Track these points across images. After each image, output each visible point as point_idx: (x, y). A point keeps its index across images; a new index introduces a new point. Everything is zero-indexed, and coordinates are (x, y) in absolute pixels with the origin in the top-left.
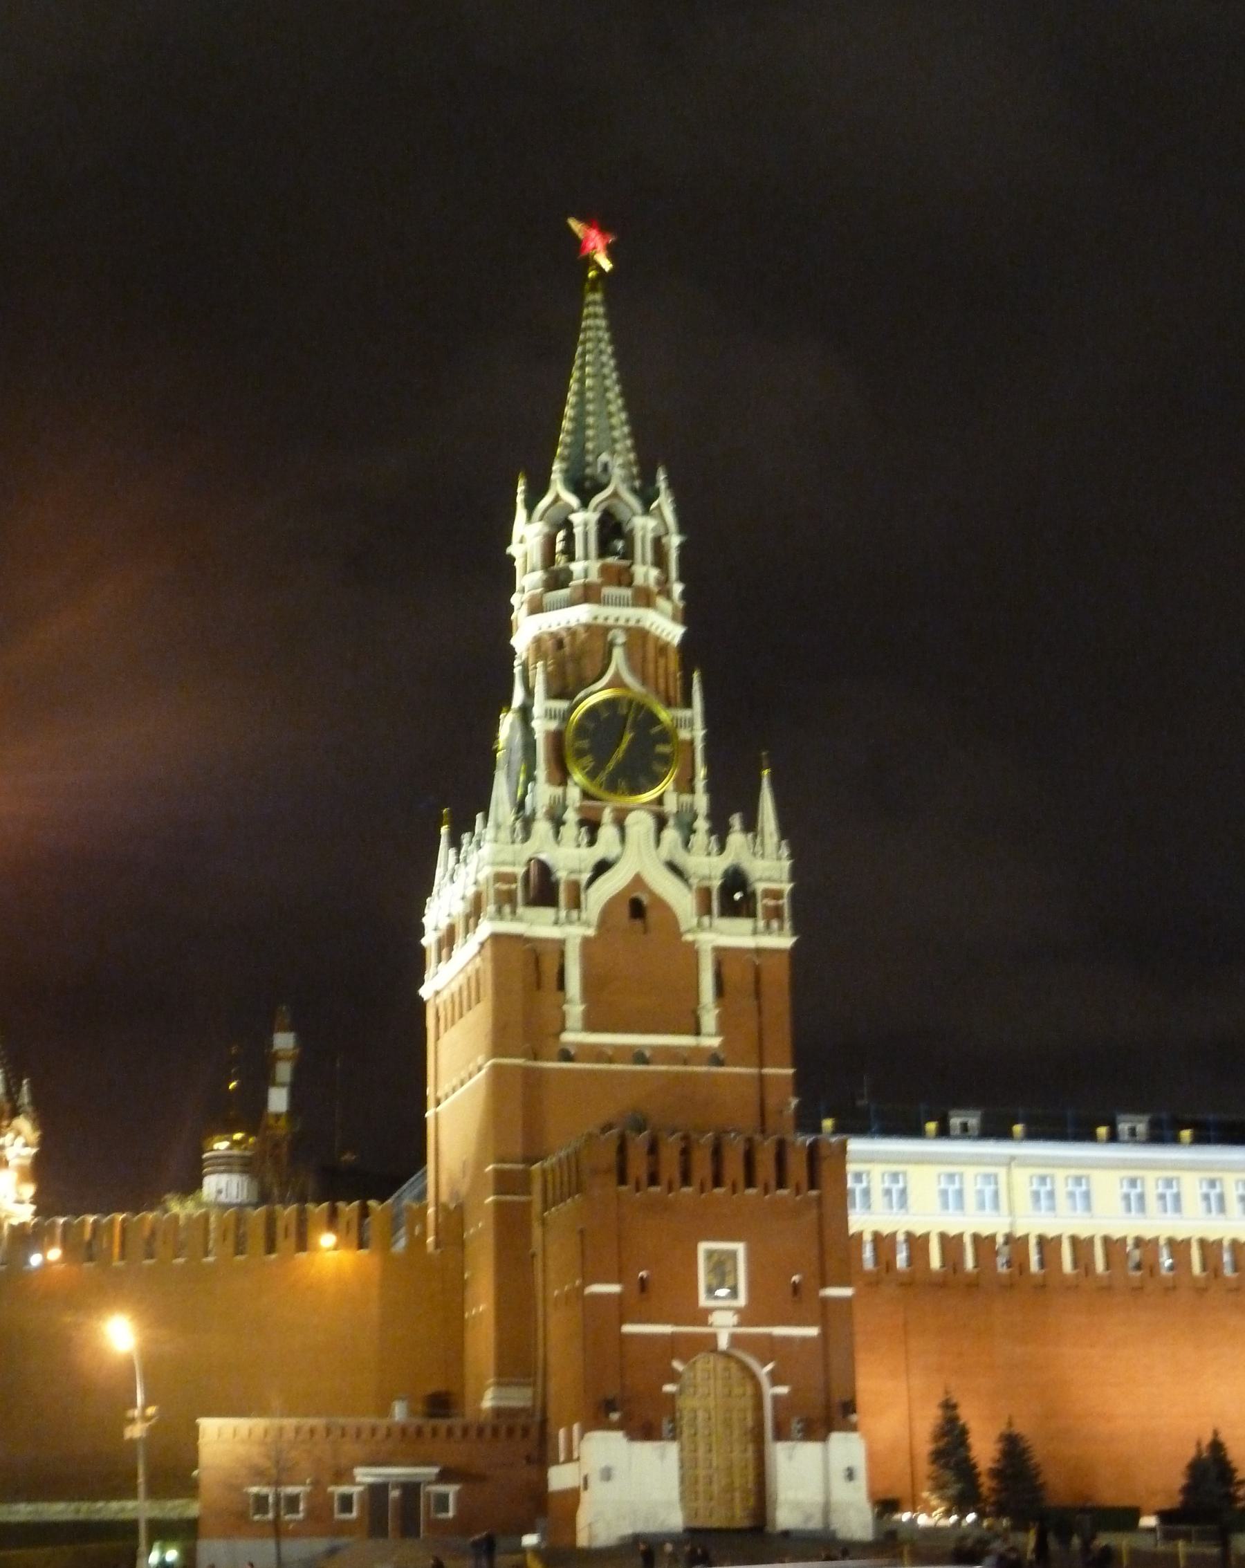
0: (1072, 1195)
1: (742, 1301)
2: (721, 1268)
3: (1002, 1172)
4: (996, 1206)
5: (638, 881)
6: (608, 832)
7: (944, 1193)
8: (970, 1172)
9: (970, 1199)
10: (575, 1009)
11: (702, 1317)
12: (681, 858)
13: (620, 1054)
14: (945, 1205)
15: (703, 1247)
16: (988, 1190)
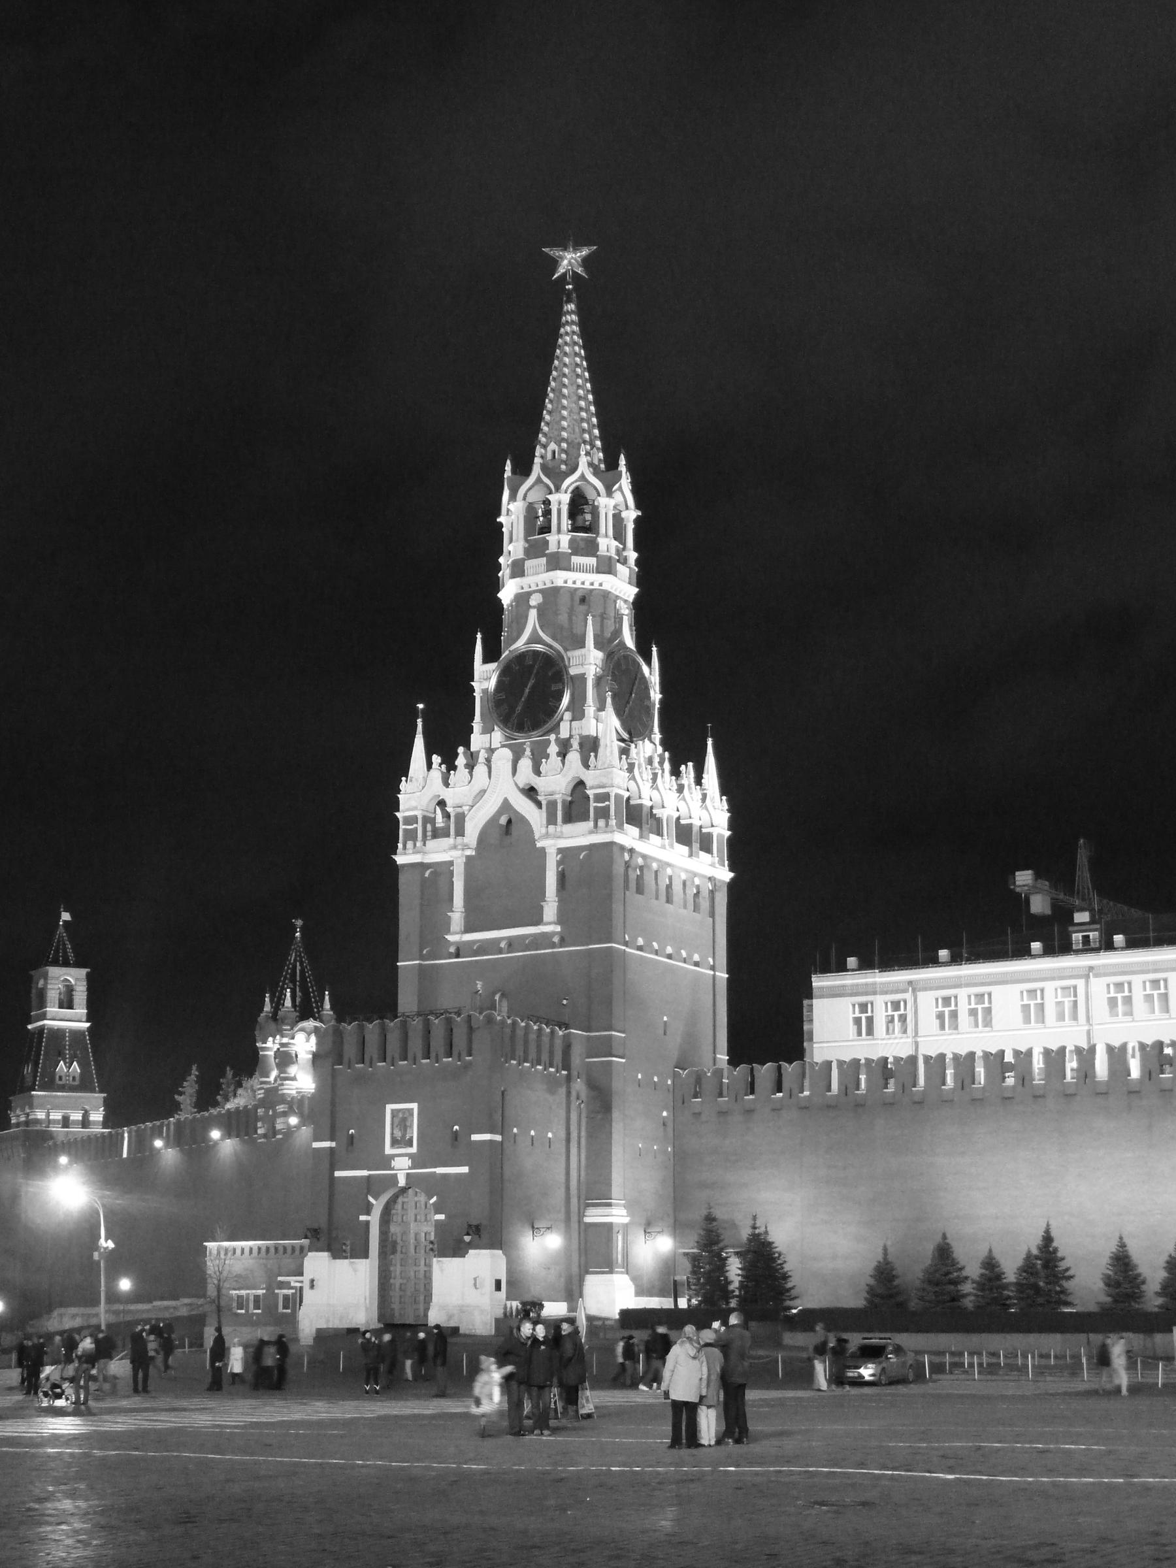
0: (1149, 998)
1: (414, 1150)
2: (402, 1121)
3: (1080, 984)
4: (1075, 1017)
5: (506, 806)
6: (481, 769)
7: (1026, 1008)
8: (1050, 987)
9: (1050, 1011)
10: (457, 917)
11: (386, 1162)
12: (539, 783)
13: (512, 943)
14: (1027, 1020)
15: (389, 1107)
16: (1067, 1002)
